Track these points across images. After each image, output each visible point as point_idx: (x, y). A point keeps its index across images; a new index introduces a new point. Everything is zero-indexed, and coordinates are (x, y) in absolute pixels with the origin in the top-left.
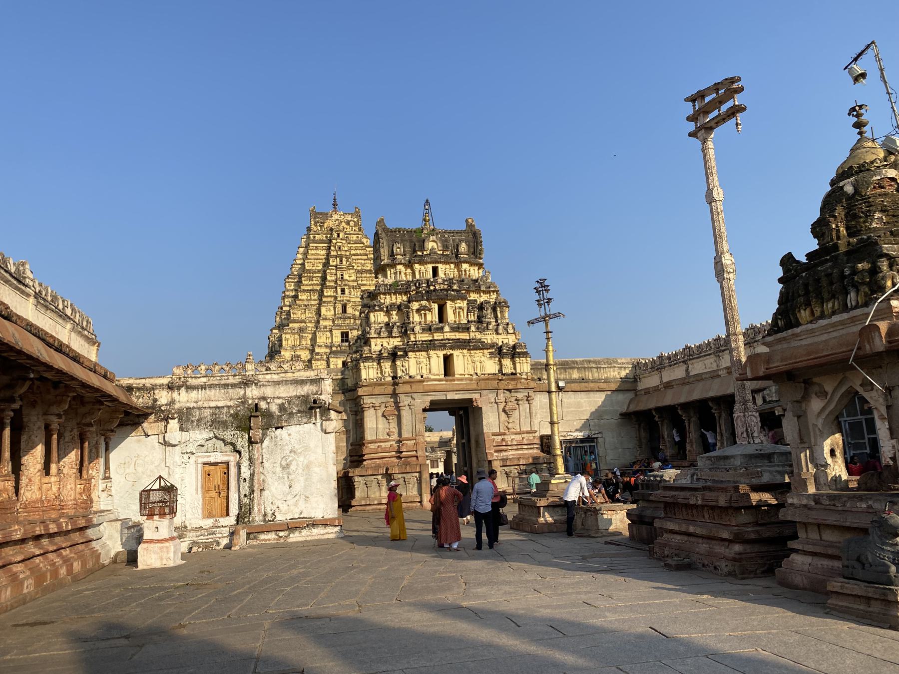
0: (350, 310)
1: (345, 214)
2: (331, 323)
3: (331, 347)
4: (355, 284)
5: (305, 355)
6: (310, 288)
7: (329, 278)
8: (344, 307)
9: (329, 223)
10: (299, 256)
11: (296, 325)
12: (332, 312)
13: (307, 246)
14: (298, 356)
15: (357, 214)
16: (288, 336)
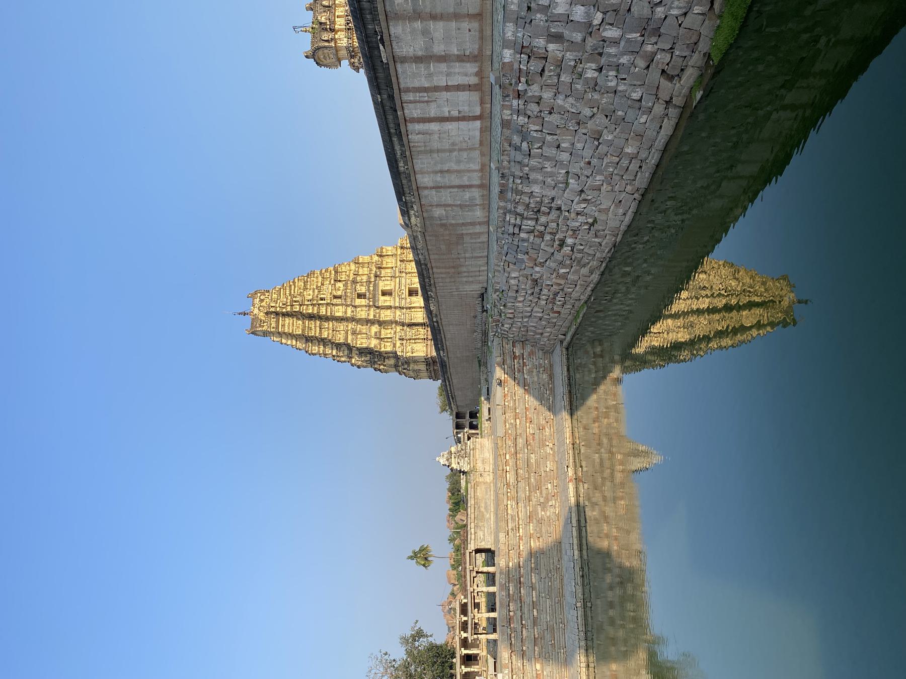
0: (339, 293)
1: (253, 305)
2: (349, 310)
3: (370, 306)
4: (316, 291)
5: (375, 329)
6: (318, 329)
7: (310, 311)
8: (335, 297)
9: (262, 316)
10: (289, 342)
11: (350, 337)
12: (340, 307)
13: (280, 334)
14: (376, 333)
15: (253, 296)
16: (359, 342)
